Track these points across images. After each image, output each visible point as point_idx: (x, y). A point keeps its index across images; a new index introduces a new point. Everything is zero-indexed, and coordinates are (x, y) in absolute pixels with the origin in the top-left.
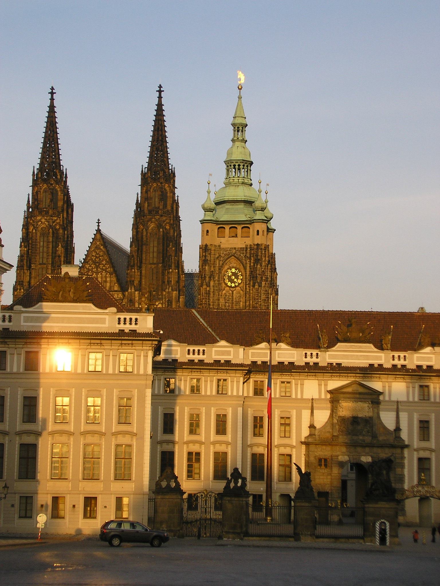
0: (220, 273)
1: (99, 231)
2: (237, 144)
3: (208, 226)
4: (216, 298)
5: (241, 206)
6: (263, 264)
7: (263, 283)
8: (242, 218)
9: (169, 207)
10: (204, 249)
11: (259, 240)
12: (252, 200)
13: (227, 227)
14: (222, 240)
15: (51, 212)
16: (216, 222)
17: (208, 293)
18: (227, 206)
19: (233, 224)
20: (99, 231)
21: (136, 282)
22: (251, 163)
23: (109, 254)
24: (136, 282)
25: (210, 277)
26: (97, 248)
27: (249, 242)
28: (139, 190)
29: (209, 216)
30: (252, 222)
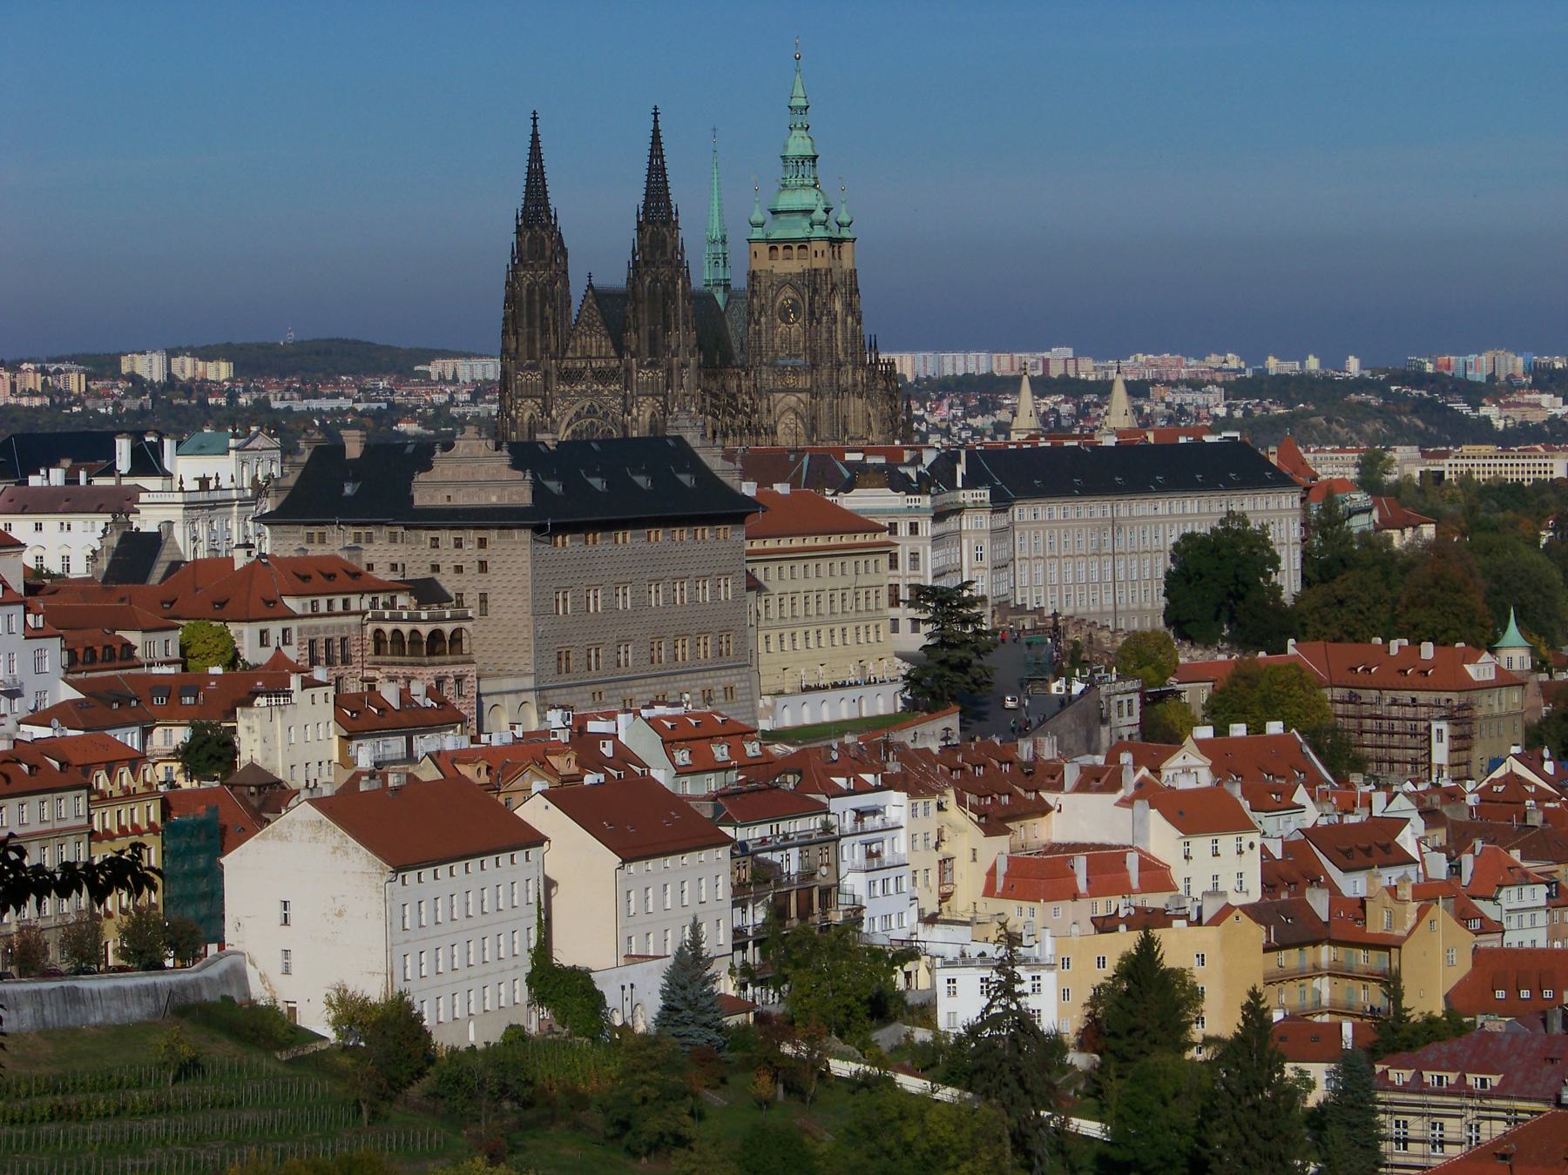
0: (773, 306)
1: (590, 286)
2: (795, 132)
3: (755, 246)
4: (770, 336)
5: (798, 217)
6: (824, 293)
7: (825, 318)
8: (799, 234)
9: (669, 255)
10: (753, 276)
11: (820, 263)
12: (813, 207)
13: (780, 247)
14: (774, 262)
15: (536, 266)
16: (767, 241)
17: (759, 333)
18: (782, 217)
19: (788, 243)
20: (590, 286)
21: (633, 348)
22: (816, 157)
23: (603, 315)
24: (633, 348)
25: (760, 313)
26: (590, 307)
27: (806, 265)
28: (635, 234)
29: (758, 233)
30: (809, 240)
